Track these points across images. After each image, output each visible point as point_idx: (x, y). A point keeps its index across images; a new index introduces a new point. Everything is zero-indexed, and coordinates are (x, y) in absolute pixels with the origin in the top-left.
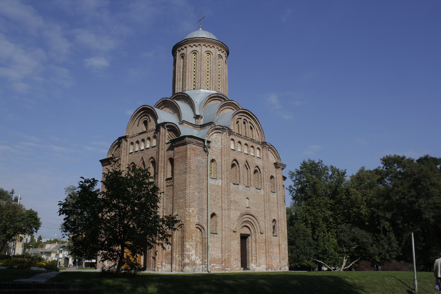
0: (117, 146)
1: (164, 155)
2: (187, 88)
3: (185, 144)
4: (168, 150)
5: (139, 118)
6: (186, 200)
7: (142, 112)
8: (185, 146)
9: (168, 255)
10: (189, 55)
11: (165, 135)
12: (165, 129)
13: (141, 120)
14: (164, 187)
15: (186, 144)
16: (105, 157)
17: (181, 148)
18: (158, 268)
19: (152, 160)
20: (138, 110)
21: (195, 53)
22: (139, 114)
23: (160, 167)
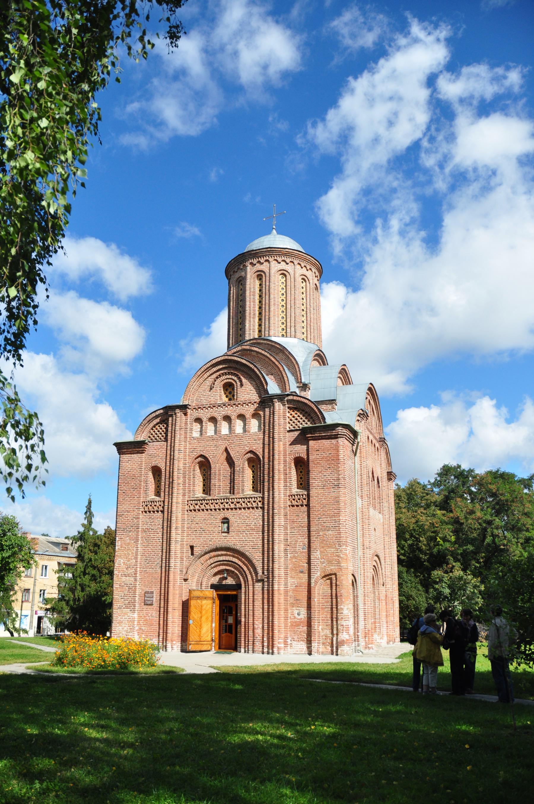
0: (158, 420)
1: (285, 451)
2: (272, 333)
3: (336, 437)
4: (293, 443)
5: (214, 376)
6: (339, 533)
7: (221, 367)
8: (334, 441)
9: (298, 625)
10: (275, 276)
11: (284, 416)
12: (284, 405)
13: (218, 380)
14: (285, 508)
15: (337, 438)
16: (129, 437)
17: (326, 443)
18: (279, 648)
19: (250, 455)
20: (214, 362)
21: (284, 274)
22: (215, 369)
23: (276, 472)
